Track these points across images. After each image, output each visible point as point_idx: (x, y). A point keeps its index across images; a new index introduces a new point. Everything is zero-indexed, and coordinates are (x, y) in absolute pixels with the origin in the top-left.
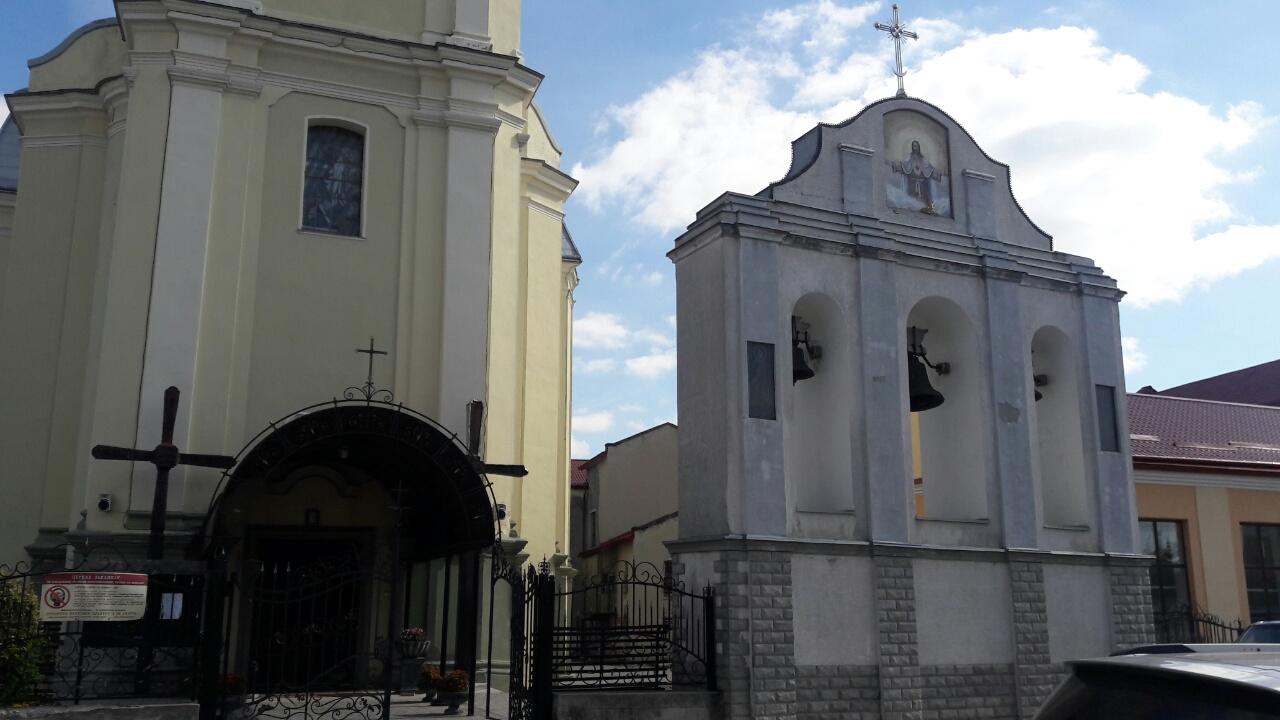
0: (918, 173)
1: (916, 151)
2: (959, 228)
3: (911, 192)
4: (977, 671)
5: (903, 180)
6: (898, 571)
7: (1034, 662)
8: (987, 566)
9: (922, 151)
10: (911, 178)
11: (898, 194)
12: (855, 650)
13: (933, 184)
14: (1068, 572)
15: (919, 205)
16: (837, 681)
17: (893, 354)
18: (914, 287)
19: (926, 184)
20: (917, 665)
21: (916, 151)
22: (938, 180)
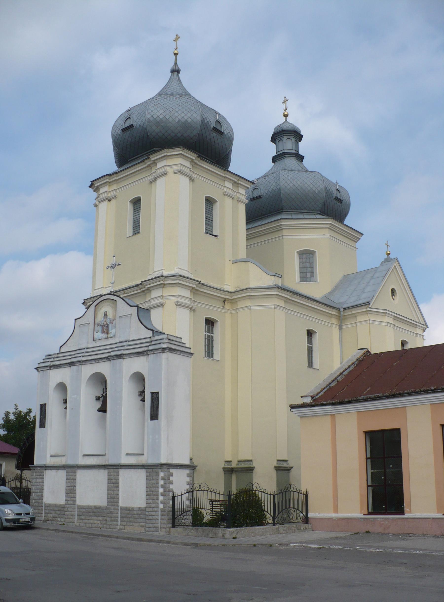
0: (105, 323)
1: (106, 315)
2: (117, 340)
3: (103, 332)
4: (96, 508)
5: (100, 328)
6: (72, 474)
7: (112, 506)
8: (102, 471)
9: (107, 314)
10: (102, 326)
11: (99, 335)
12: (61, 500)
13: (110, 326)
14: (132, 472)
15: (104, 336)
16: (55, 509)
17: (78, 398)
18: (88, 370)
19: (108, 327)
20: (75, 504)
21: (106, 315)
22: (112, 323)
